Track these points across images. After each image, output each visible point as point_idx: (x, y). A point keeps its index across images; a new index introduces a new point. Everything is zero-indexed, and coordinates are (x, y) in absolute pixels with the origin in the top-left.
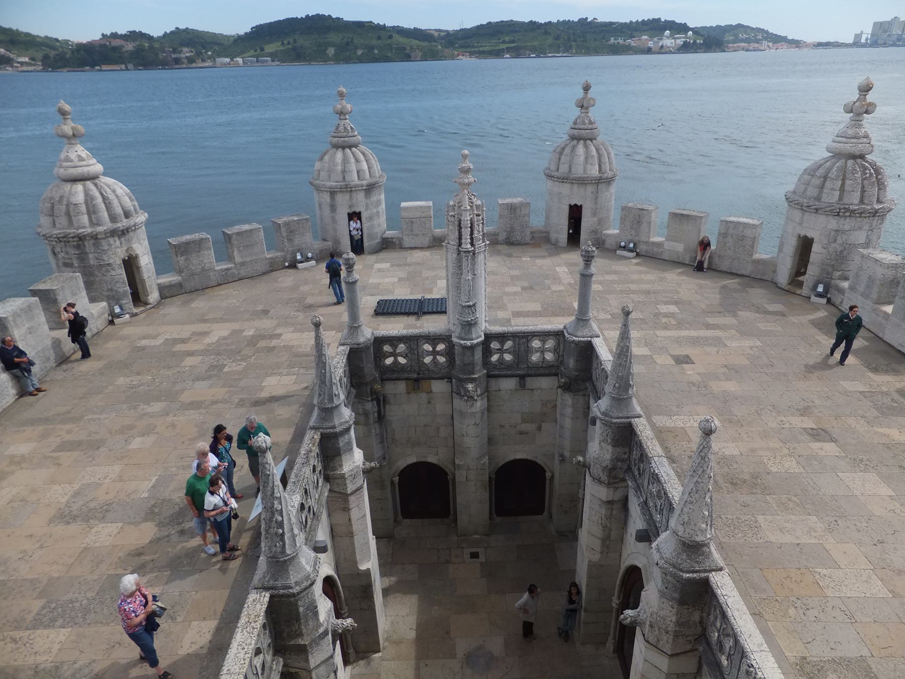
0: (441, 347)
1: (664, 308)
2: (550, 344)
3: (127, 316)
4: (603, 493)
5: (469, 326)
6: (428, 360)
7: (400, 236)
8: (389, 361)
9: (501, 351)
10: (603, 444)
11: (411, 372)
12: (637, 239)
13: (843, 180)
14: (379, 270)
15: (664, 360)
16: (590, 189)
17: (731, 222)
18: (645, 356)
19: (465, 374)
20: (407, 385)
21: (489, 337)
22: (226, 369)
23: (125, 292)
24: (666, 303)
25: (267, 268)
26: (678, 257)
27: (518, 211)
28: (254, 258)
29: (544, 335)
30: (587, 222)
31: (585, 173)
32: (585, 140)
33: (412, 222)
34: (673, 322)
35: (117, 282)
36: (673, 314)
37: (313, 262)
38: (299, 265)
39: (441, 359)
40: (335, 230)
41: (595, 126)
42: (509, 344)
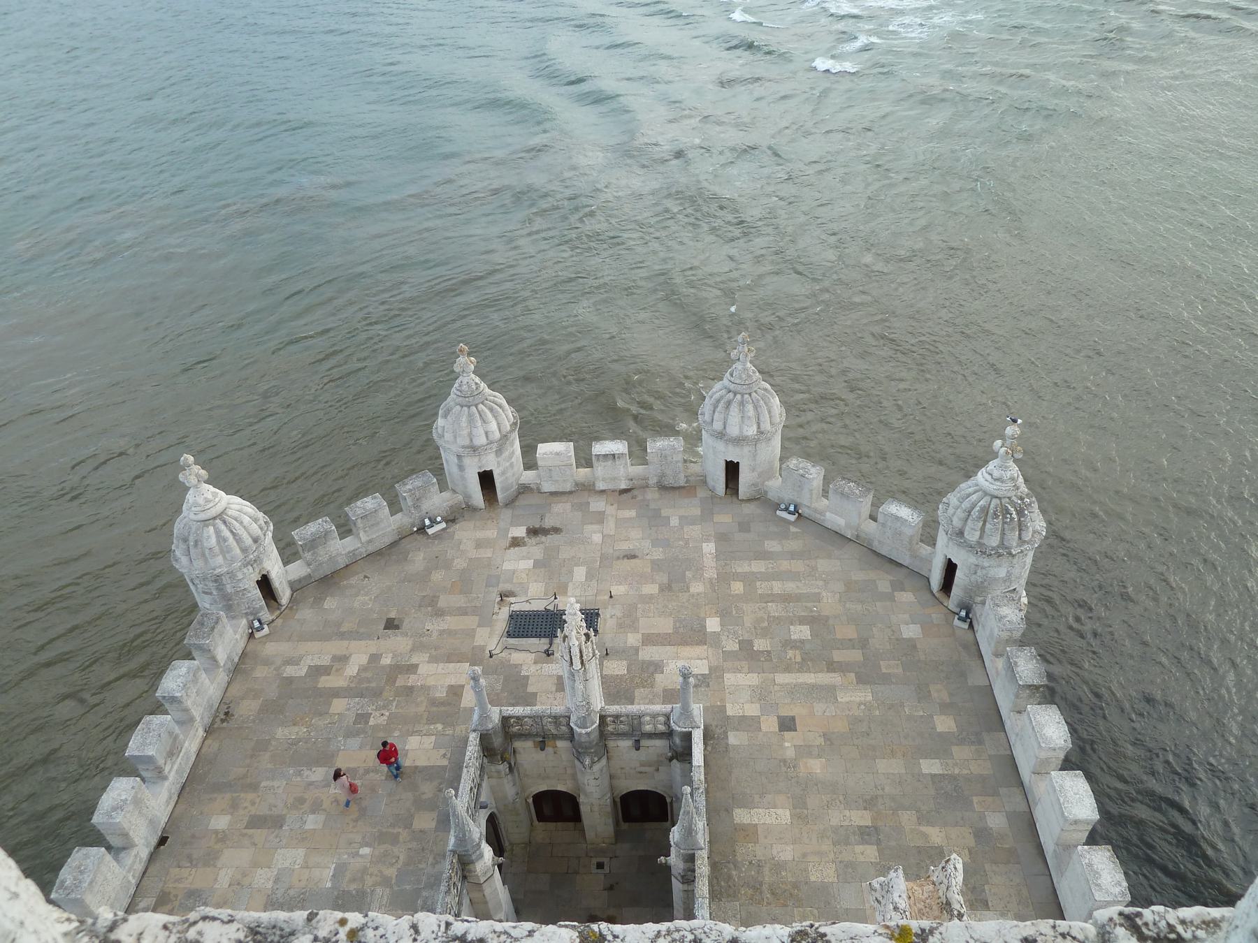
12: (798, 500)
16: (746, 449)
24: (802, 621)
36: (802, 642)
38: (430, 531)
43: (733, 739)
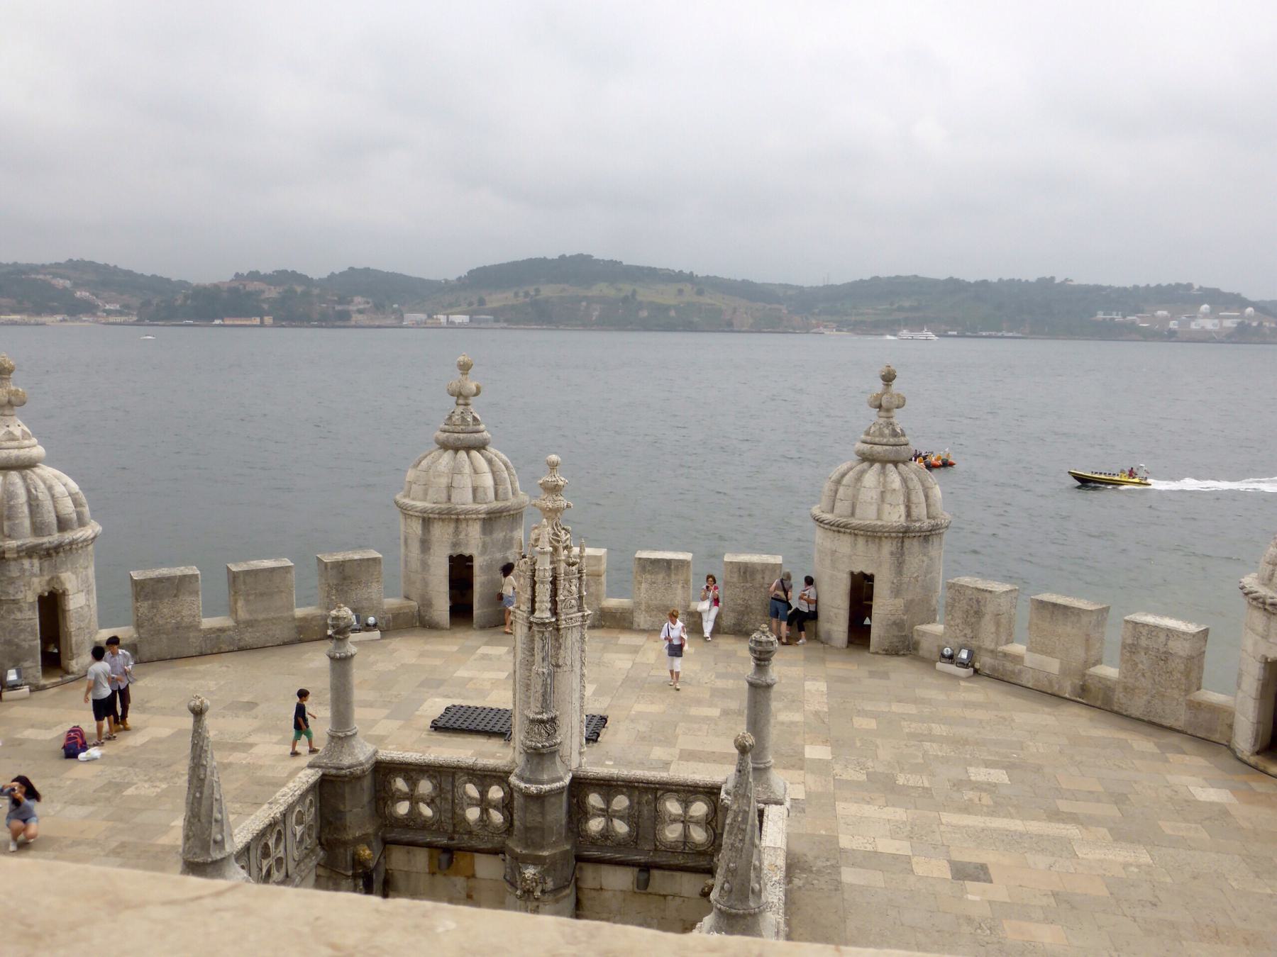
0: (496, 793)
1: (979, 774)
2: (699, 809)
3: (26, 689)
5: (539, 756)
6: (473, 814)
8: (403, 808)
9: (607, 814)
11: (440, 831)
12: (974, 643)
14: (485, 657)
15: (941, 869)
16: (887, 547)
17: (1144, 625)
18: (895, 857)
19: (527, 846)
20: (431, 857)
21: (580, 785)
22: (130, 791)
23: (32, 648)
24: (988, 764)
25: (288, 634)
26: (1050, 682)
27: (759, 577)
29: (688, 792)
30: (883, 606)
31: (879, 518)
32: (884, 462)
34: (987, 799)
35: (22, 631)
36: (995, 785)
37: (376, 634)
39: (497, 817)
40: (425, 583)
41: (903, 440)
42: (621, 802)
43: (848, 876)
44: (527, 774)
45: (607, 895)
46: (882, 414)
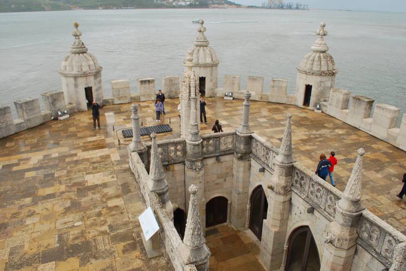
4: (281, 198)
7: (113, 98)
10: (280, 177)
13: (321, 61)
16: (209, 69)
27: (173, 82)
28: (35, 116)
30: (208, 85)
32: (203, 46)
33: (119, 91)
37: (68, 116)
38: (61, 118)
39: (179, 153)
44: (193, 139)
45: (208, 166)
46: (201, 33)
